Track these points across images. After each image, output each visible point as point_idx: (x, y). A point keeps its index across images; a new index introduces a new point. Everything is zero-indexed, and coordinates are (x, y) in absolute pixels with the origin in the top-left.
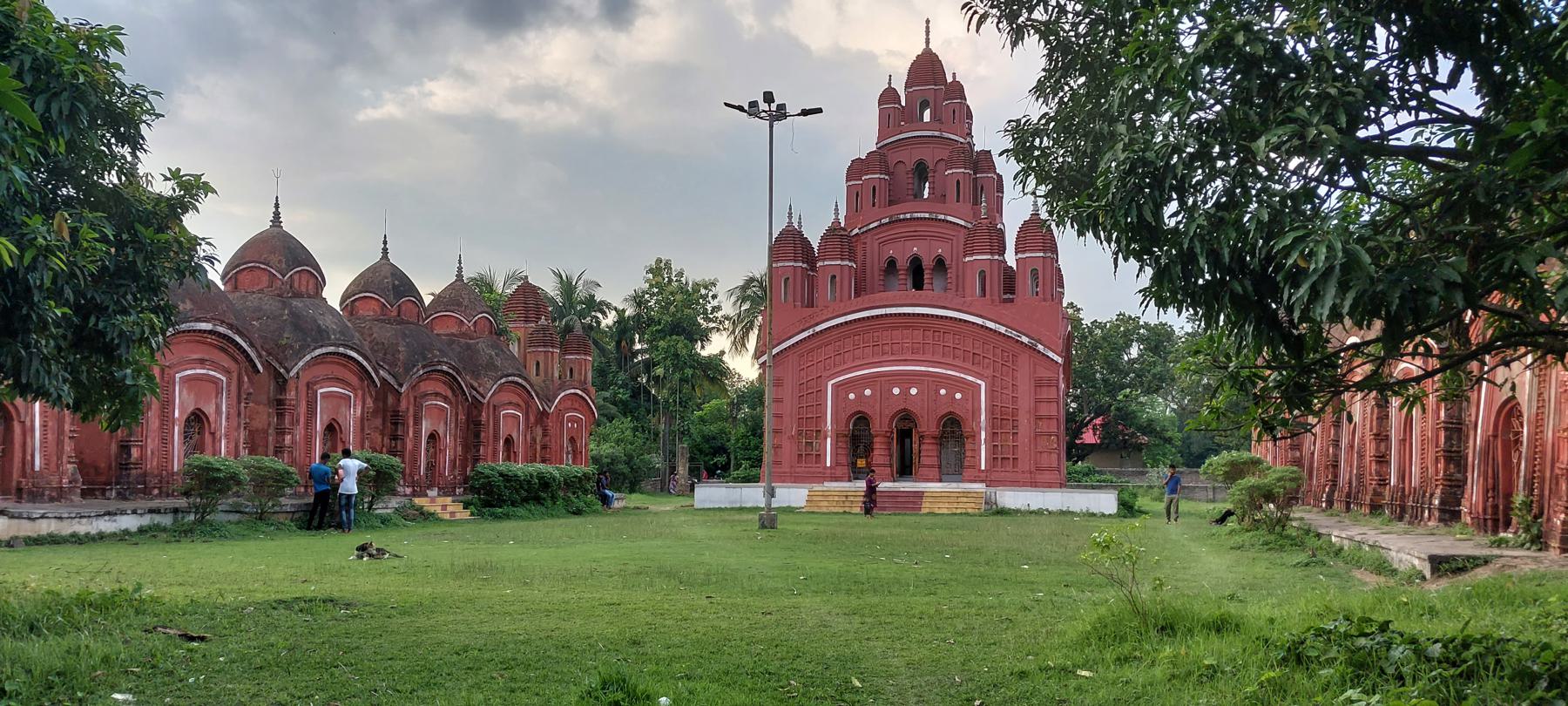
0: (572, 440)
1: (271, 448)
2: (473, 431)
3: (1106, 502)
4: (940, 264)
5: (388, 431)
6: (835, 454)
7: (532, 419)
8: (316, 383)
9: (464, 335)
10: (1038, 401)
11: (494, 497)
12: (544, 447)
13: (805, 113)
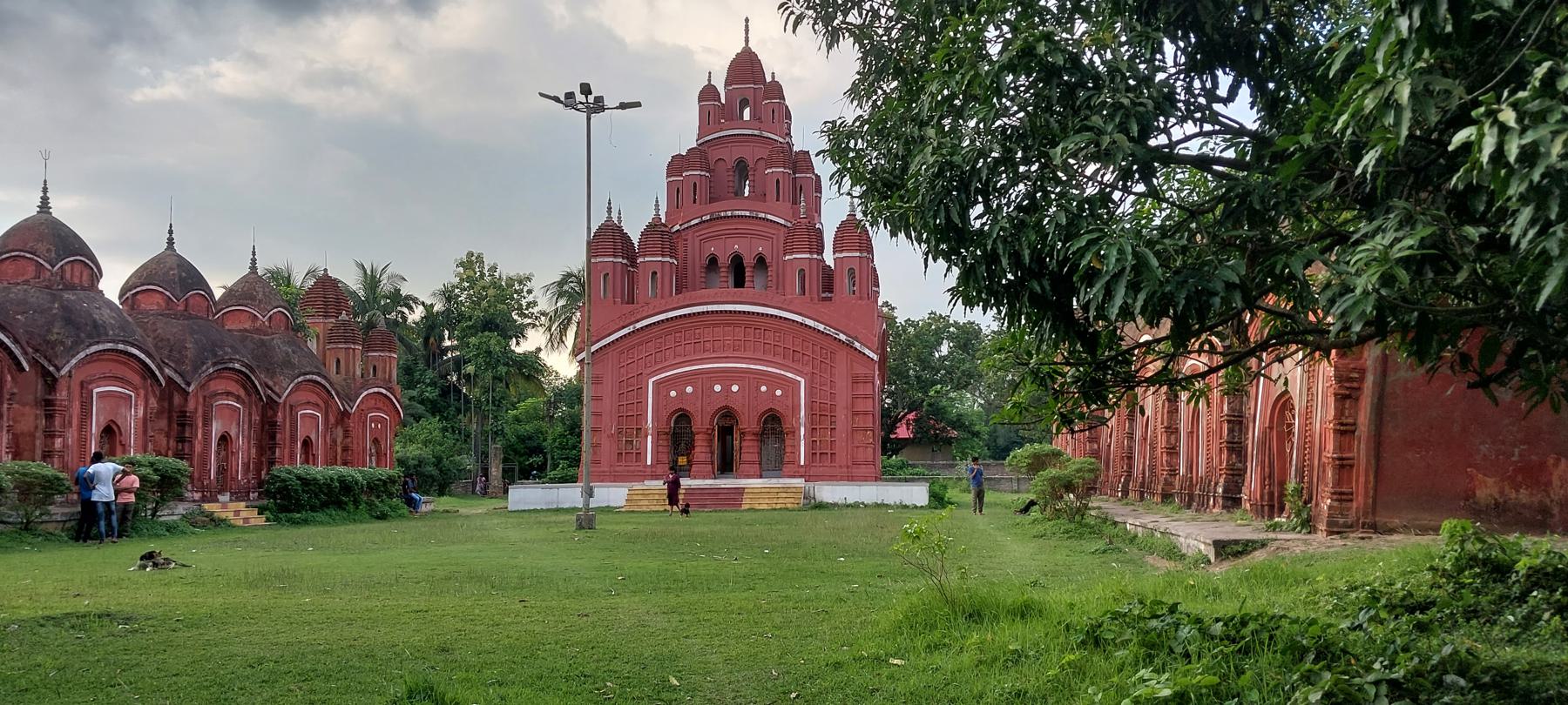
0: (376, 441)
1: (39, 452)
2: (267, 433)
3: (917, 494)
4: (761, 262)
5: (174, 433)
6: (656, 452)
7: (332, 420)
8: (91, 382)
9: (258, 331)
10: (855, 397)
11: (290, 502)
12: (345, 449)
13: (623, 106)
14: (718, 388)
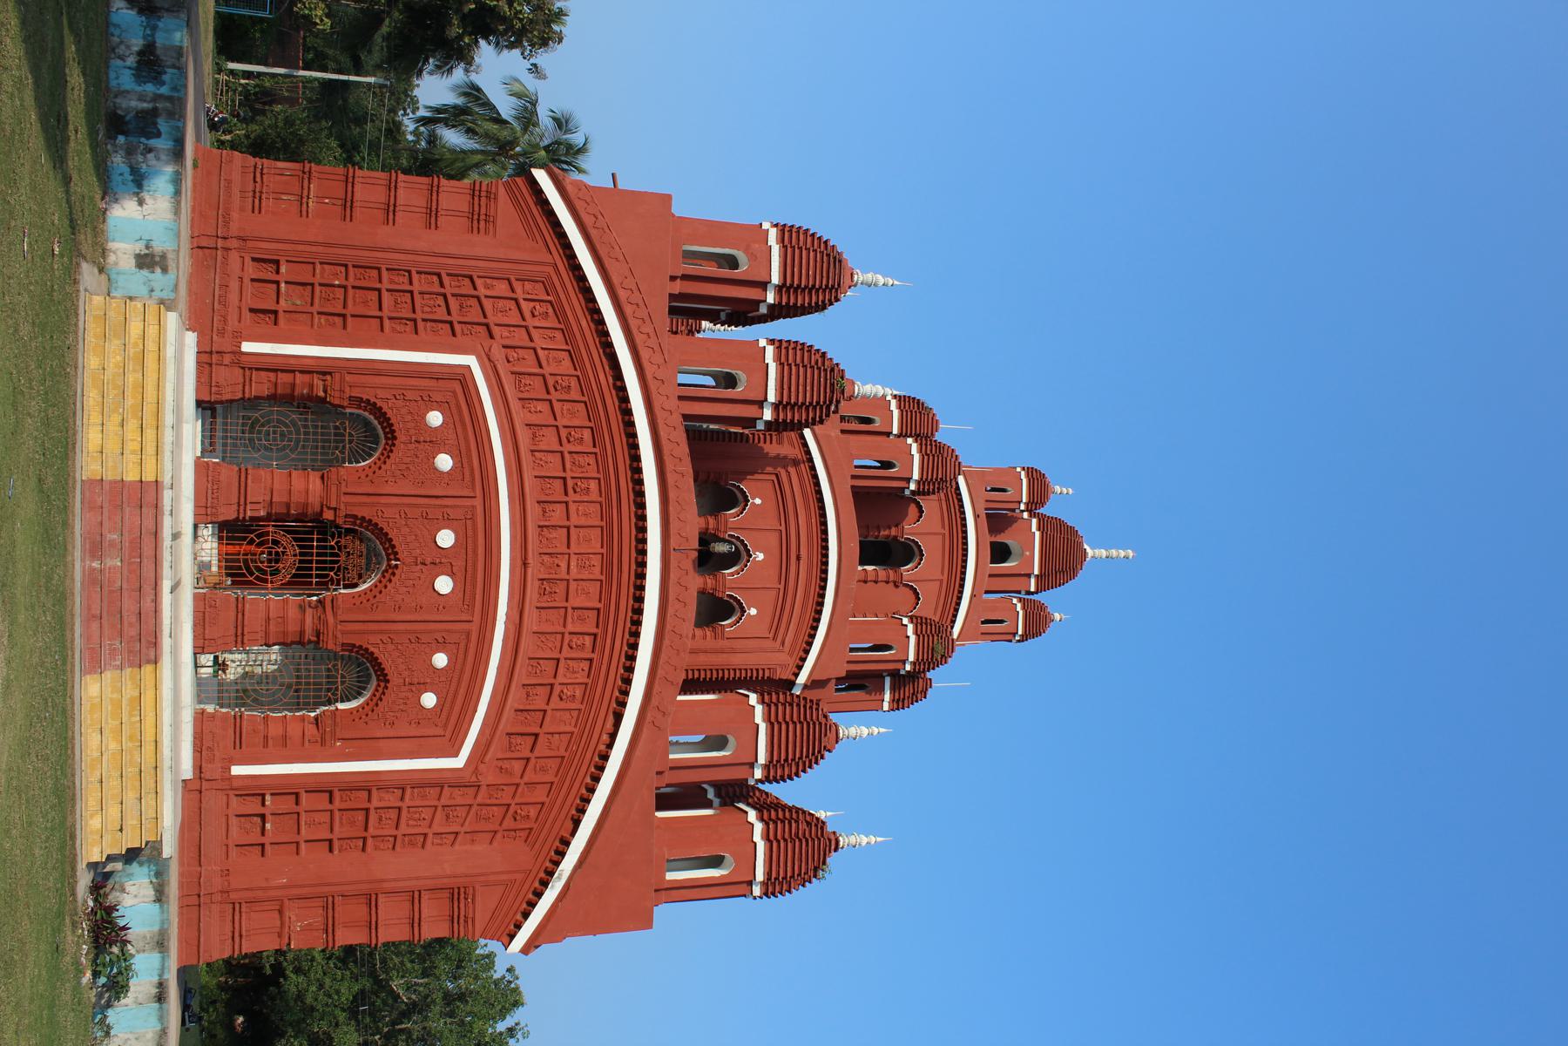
10: (414, 897)
14: (446, 538)
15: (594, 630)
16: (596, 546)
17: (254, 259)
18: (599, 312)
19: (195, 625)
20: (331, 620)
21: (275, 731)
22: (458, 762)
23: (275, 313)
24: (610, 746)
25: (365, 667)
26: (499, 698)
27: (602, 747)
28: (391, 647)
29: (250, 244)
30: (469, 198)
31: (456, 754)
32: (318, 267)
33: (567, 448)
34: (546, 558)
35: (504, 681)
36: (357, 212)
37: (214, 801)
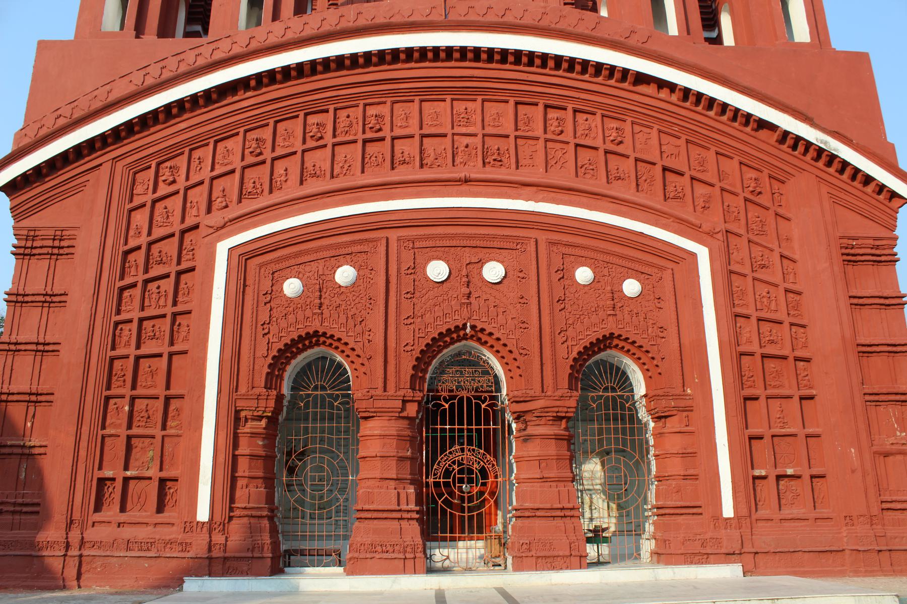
14: (437, 270)
15: (541, 107)
16: (443, 108)
17: (98, 509)
18: (168, 107)
19: (553, 568)
20: (540, 403)
21: (676, 467)
22: (703, 253)
23: (163, 482)
24: (672, 87)
25: (592, 372)
26: (624, 209)
27: (674, 98)
28: (571, 332)
29: (77, 515)
30: (33, 261)
31: (694, 255)
32: (108, 431)
33: (329, 139)
34: (458, 160)
35: (604, 203)
36: (43, 388)
37: (765, 537)
